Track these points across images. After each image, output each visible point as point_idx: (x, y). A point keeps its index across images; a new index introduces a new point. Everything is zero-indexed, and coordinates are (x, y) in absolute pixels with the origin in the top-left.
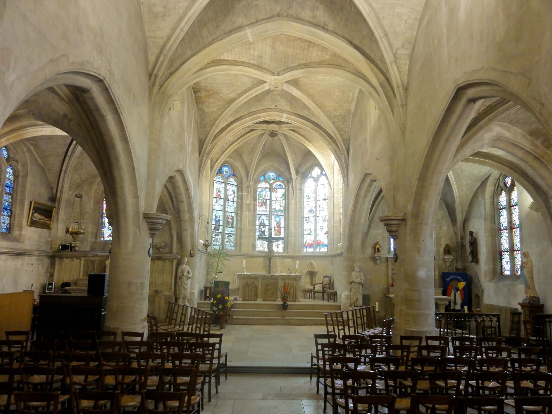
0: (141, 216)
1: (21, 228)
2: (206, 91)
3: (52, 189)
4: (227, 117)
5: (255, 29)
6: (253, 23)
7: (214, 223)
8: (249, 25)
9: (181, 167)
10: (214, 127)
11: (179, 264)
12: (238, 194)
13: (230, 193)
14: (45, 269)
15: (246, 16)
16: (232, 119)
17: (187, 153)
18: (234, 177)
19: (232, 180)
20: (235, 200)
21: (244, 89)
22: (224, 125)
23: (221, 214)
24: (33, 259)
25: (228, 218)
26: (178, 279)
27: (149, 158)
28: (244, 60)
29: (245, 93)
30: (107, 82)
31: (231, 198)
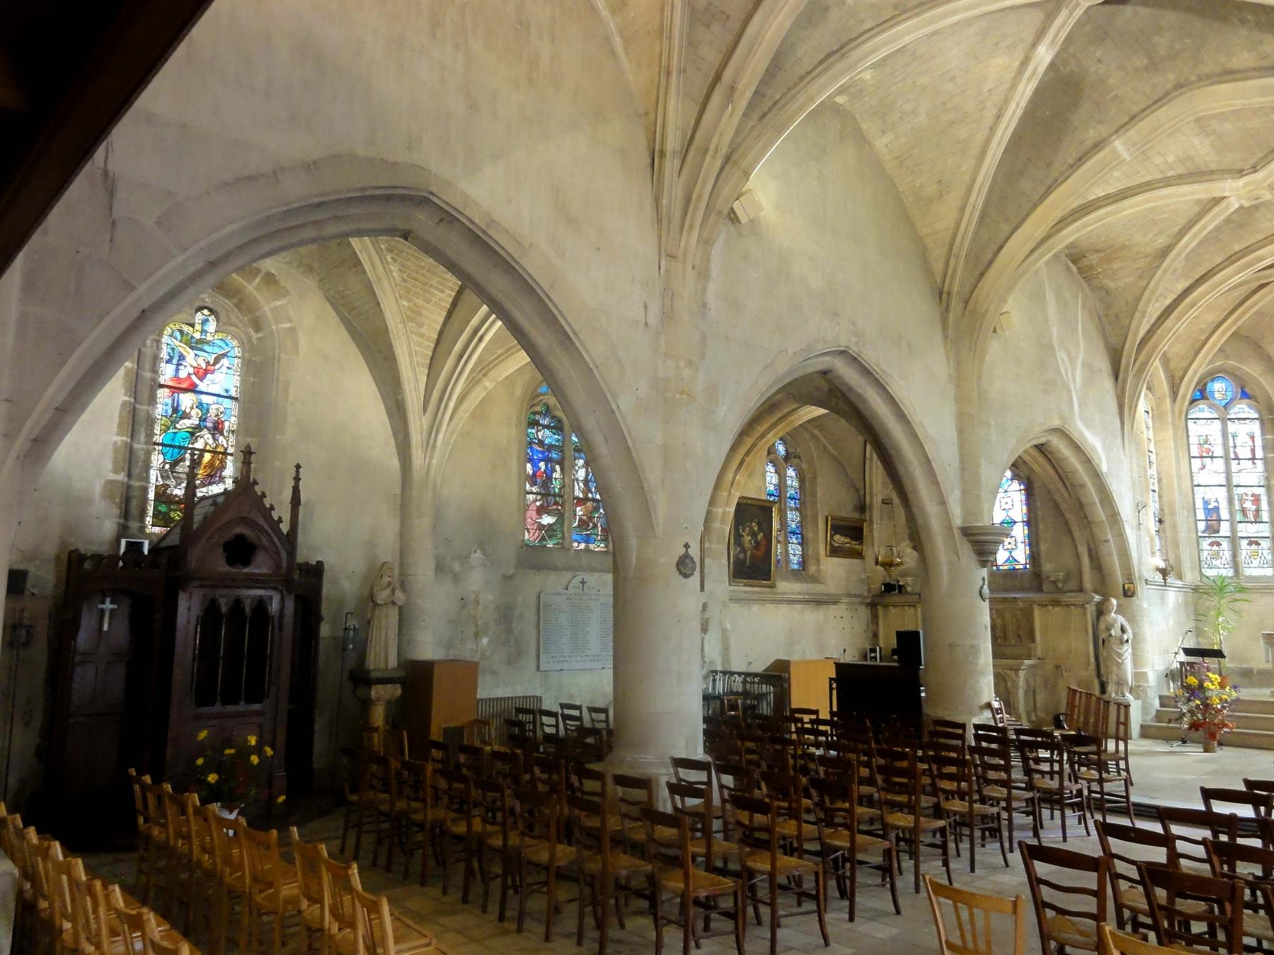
0: (957, 533)
1: (818, 561)
2: (1098, 251)
3: (857, 490)
4: (1167, 285)
5: (1131, 132)
6: (1126, 124)
7: (1201, 514)
8: (1117, 131)
9: (1055, 422)
10: (1137, 315)
11: (1101, 612)
12: (1264, 440)
13: (1243, 439)
14: (864, 627)
15: (1100, 122)
16: (1181, 286)
17: (1069, 391)
18: (1247, 401)
19: (1243, 409)
21: (1182, 221)
22: (1168, 302)
23: (1221, 493)
24: (840, 610)
25: (1241, 500)
26: (1102, 644)
27: (961, 431)
28: (1149, 178)
29: (1190, 228)
30: (854, 350)
31: (1244, 452)
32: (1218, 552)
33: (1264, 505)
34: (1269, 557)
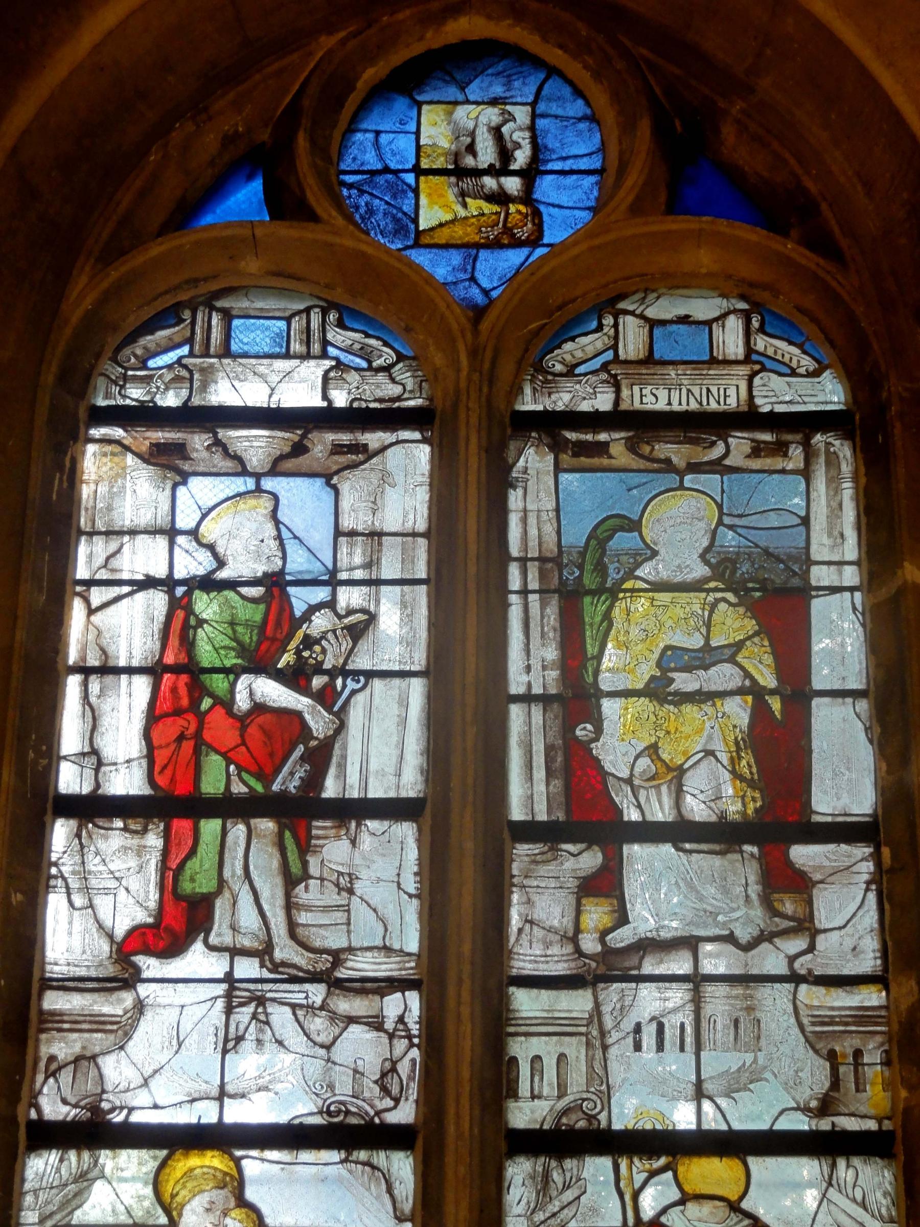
20: (845, 775)
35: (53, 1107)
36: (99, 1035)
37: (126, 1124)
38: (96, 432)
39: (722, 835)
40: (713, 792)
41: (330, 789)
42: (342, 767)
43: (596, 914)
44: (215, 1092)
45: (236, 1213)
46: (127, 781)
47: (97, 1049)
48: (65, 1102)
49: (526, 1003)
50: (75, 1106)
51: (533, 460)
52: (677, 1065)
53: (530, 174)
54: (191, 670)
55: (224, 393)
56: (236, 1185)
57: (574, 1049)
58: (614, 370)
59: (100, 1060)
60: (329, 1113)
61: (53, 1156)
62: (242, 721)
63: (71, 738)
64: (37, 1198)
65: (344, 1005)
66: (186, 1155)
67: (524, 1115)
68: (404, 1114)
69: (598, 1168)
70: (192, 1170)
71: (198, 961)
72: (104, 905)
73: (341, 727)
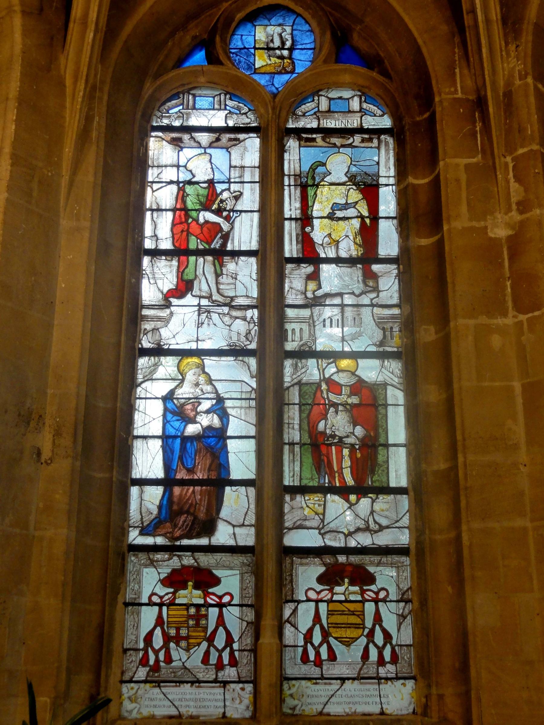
12: (404, 196)
23: (234, 378)
31: (336, 236)
32: (199, 614)
33: (397, 428)
34: (405, 635)
35: (146, 344)
36: (159, 322)
37: (168, 349)
38: (153, 134)
39: (351, 261)
40: (349, 248)
41: (229, 247)
42: (233, 240)
43: (312, 286)
44: (195, 339)
45: (203, 375)
46: (166, 245)
47: (159, 327)
48: (149, 342)
49: (290, 313)
50: (153, 344)
51: (292, 144)
52: (337, 331)
53: (291, 50)
54: (185, 210)
55: (195, 121)
56: (202, 367)
57: (305, 327)
58: (318, 114)
59: (160, 330)
60: (230, 346)
61: (147, 358)
62: (202, 226)
63: (148, 231)
64: (142, 371)
65: (235, 313)
66: (187, 358)
67: (290, 346)
68: (253, 346)
69: (312, 362)
70: (189, 363)
71: (189, 299)
72: (160, 283)
73: (232, 228)
